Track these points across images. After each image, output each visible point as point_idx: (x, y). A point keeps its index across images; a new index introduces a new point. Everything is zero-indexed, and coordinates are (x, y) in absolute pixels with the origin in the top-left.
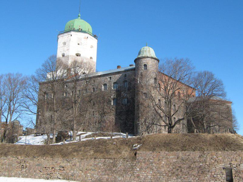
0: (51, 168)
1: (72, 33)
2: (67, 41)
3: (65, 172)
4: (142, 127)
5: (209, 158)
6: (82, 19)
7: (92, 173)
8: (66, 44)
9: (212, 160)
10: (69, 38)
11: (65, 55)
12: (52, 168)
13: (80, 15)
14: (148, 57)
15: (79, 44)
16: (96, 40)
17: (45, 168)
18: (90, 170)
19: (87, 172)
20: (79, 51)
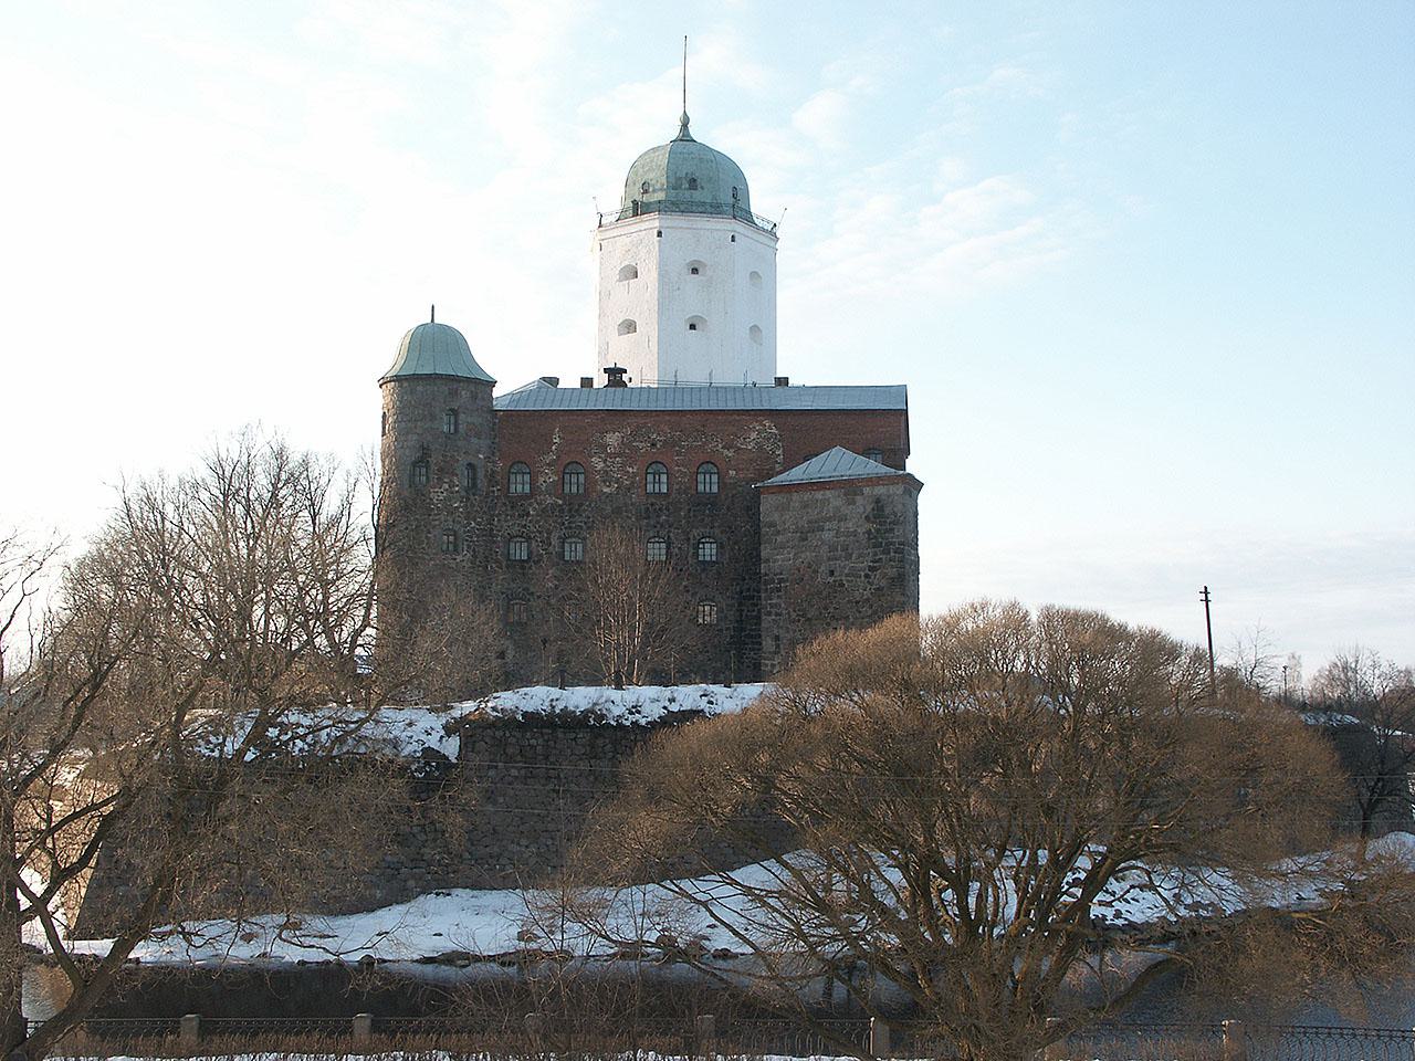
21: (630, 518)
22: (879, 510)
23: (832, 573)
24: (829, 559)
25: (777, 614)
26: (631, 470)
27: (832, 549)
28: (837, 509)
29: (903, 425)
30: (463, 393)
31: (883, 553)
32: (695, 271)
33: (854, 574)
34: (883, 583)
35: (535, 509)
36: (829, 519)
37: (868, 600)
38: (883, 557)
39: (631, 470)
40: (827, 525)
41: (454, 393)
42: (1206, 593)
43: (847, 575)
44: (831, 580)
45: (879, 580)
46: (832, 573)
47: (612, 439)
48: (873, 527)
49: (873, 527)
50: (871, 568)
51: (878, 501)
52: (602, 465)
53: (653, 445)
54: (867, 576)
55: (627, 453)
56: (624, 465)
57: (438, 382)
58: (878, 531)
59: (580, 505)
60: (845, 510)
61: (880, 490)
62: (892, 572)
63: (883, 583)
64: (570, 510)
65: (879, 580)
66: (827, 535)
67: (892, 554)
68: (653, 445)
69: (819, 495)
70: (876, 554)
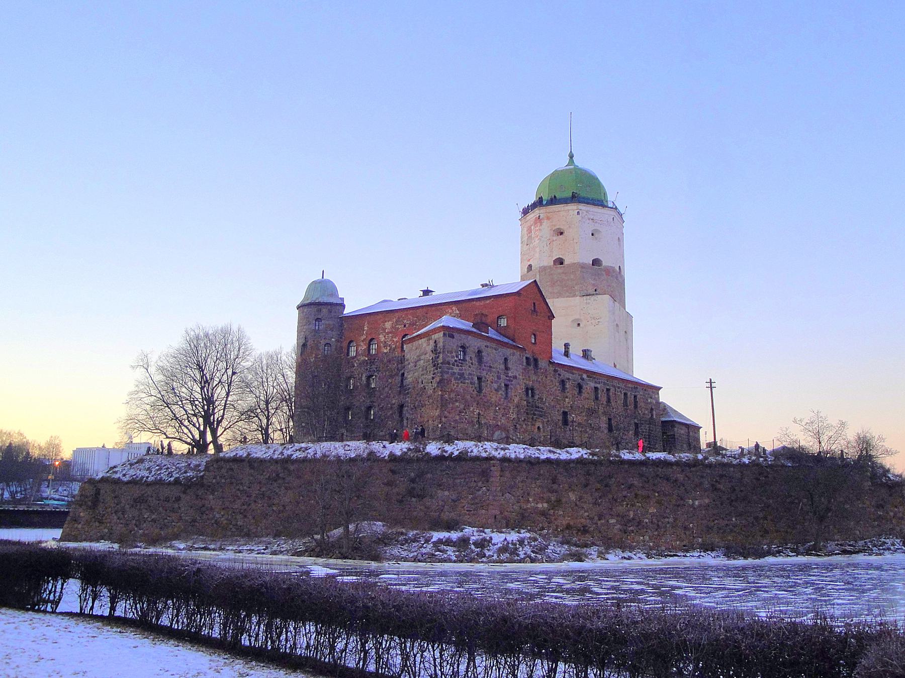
21: (394, 364)
26: (395, 340)
29: (478, 304)
30: (324, 310)
32: (562, 233)
35: (357, 363)
38: (436, 371)
39: (395, 340)
41: (320, 311)
42: (711, 382)
47: (388, 325)
48: (433, 356)
49: (433, 356)
50: (433, 378)
52: (384, 338)
53: (405, 326)
55: (395, 331)
56: (392, 337)
57: (312, 306)
59: (374, 359)
64: (370, 363)
66: (422, 362)
68: (405, 326)
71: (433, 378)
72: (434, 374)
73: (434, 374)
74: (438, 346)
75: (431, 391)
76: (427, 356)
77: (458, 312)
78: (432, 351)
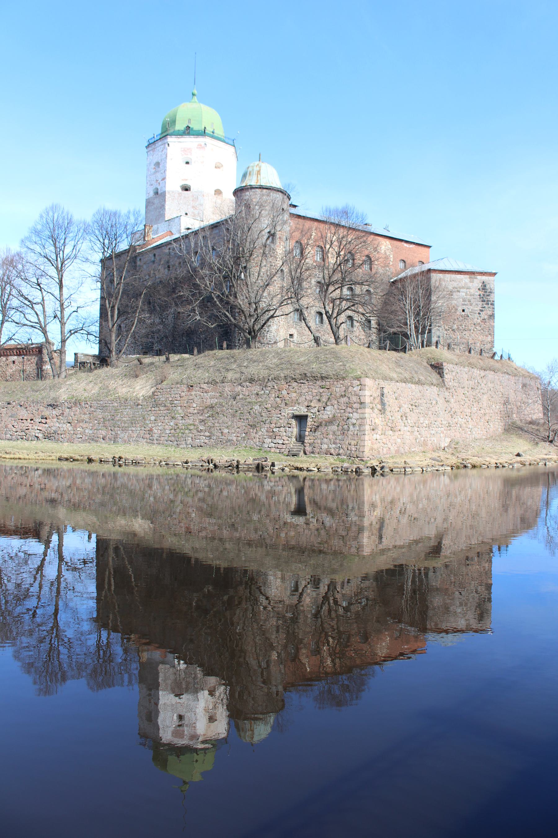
0: (29, 421)
1: (170, 139)
2: (161, 160)
3: (47, 425)
4: (239, 340)
5: (273, 395)
6: (200, 101)
7: (84, 426)
8: (161, 166)
9: (278, 399)
10: (165, 151)
11: (159, 192)
12: (31, 420)
13: (195, 92)
14: (252, 188)
15: (187, 163)
16: (232, 149)
17: (22, 420)
18: (83, 421)
19: (78, 425)
20: (186, 180)
22: (484, 287)
23: (463, 311)
24: (463, 305)
25: (439, 327)
27: (464, 301)
28: (466, 283)
31: (486, 304)
33: (473, 312)
34: (486, 317)
36: (463, 288)
37: (479, 324)
40: (461, 290)
43: (470, 312)
44: (463, 313)
45: (484, 315)
46: (463, 311)
51: (484, 282)
54: (479, 314)
58: (484, 295)
60: (470, 285)
61: (484, 278)
62: (490, 313)
63: (486, 317)
65: (484, 315)
67: (490, 305)
69: (459, 276)
70: (483, 305)
71: (482, 311)
72: (482, 308)
73: (482, 308)
74: (488, 287)
75: (479, 321)
76: (472, 291)
77: (390, 247)
78: (479, 289)
